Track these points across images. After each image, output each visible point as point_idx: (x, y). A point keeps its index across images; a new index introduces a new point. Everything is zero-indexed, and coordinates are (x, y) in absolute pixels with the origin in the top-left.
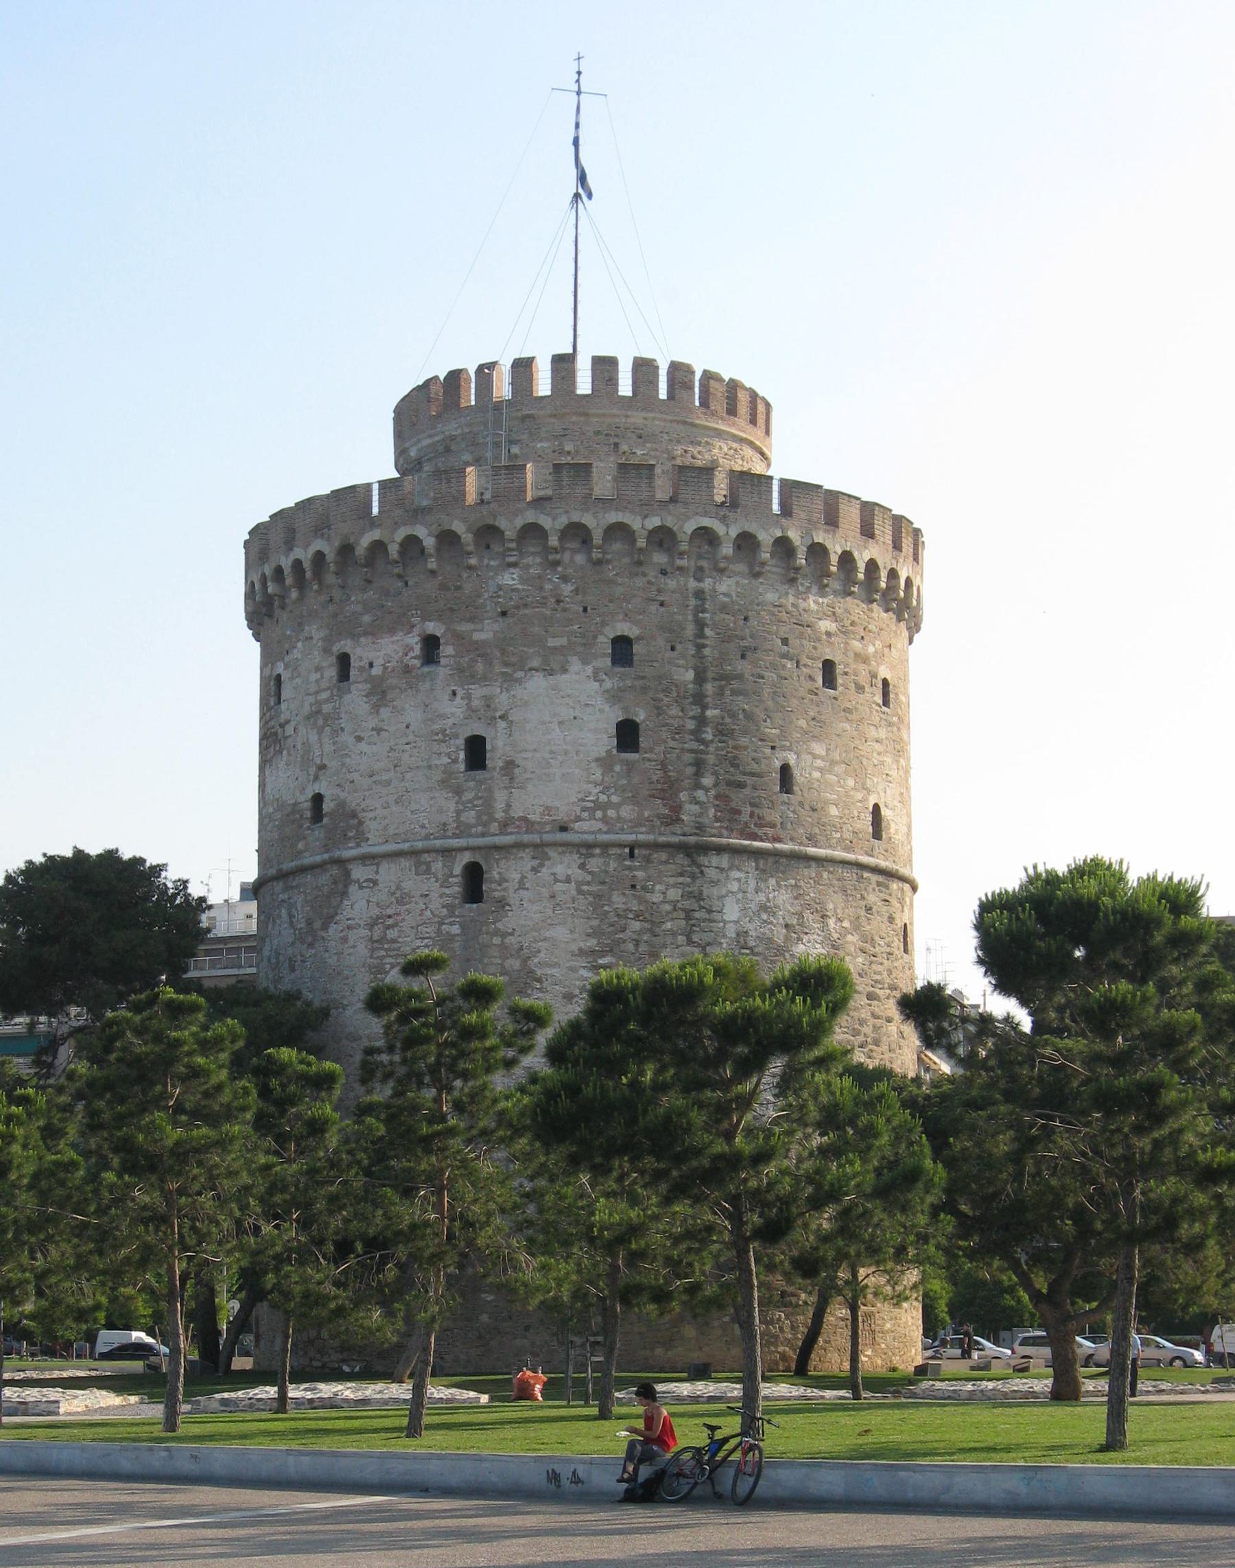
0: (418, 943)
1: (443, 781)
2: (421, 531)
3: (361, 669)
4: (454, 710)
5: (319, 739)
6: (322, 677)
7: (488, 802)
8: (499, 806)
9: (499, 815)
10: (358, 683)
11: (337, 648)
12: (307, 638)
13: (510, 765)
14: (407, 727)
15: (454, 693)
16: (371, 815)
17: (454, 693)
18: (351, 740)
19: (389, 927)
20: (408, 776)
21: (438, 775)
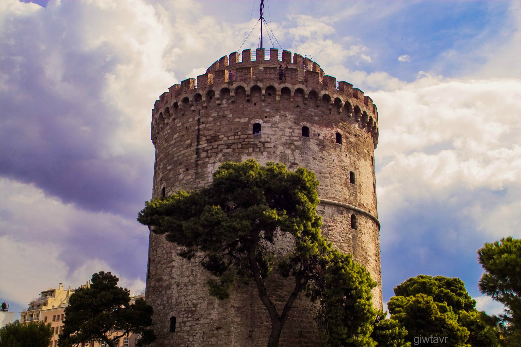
0: (340, 239)
1: (345, 184)
2: (341, 98)
3: (315, 135)
4: (347, 161)
5: (293, 154)
6: (293, 132)
7: (356, 195)
8: (358, 198)
9: (359, 201)
10: (314, 139)
11: (302, 124)
12: (282, 116)
13: (360, 185)
14: (333, 161)
15: (346, 155)
16: (321, 187)
17: (346, 155)
18: (311, 158)
19: (329, 230)
20: (334, 178)
21: (343, 181)
